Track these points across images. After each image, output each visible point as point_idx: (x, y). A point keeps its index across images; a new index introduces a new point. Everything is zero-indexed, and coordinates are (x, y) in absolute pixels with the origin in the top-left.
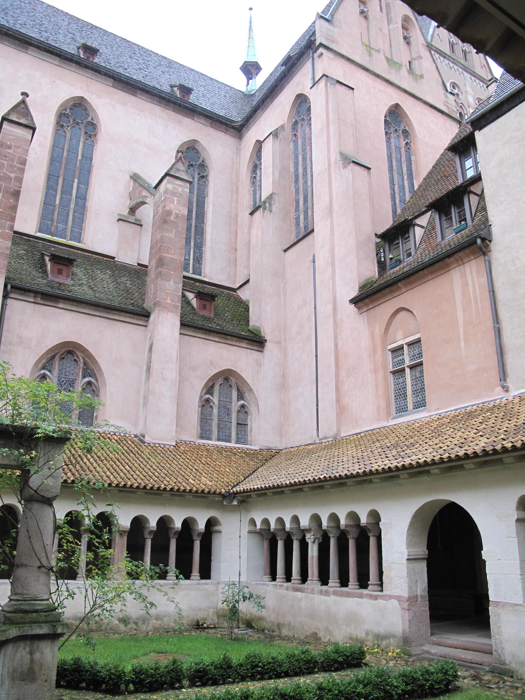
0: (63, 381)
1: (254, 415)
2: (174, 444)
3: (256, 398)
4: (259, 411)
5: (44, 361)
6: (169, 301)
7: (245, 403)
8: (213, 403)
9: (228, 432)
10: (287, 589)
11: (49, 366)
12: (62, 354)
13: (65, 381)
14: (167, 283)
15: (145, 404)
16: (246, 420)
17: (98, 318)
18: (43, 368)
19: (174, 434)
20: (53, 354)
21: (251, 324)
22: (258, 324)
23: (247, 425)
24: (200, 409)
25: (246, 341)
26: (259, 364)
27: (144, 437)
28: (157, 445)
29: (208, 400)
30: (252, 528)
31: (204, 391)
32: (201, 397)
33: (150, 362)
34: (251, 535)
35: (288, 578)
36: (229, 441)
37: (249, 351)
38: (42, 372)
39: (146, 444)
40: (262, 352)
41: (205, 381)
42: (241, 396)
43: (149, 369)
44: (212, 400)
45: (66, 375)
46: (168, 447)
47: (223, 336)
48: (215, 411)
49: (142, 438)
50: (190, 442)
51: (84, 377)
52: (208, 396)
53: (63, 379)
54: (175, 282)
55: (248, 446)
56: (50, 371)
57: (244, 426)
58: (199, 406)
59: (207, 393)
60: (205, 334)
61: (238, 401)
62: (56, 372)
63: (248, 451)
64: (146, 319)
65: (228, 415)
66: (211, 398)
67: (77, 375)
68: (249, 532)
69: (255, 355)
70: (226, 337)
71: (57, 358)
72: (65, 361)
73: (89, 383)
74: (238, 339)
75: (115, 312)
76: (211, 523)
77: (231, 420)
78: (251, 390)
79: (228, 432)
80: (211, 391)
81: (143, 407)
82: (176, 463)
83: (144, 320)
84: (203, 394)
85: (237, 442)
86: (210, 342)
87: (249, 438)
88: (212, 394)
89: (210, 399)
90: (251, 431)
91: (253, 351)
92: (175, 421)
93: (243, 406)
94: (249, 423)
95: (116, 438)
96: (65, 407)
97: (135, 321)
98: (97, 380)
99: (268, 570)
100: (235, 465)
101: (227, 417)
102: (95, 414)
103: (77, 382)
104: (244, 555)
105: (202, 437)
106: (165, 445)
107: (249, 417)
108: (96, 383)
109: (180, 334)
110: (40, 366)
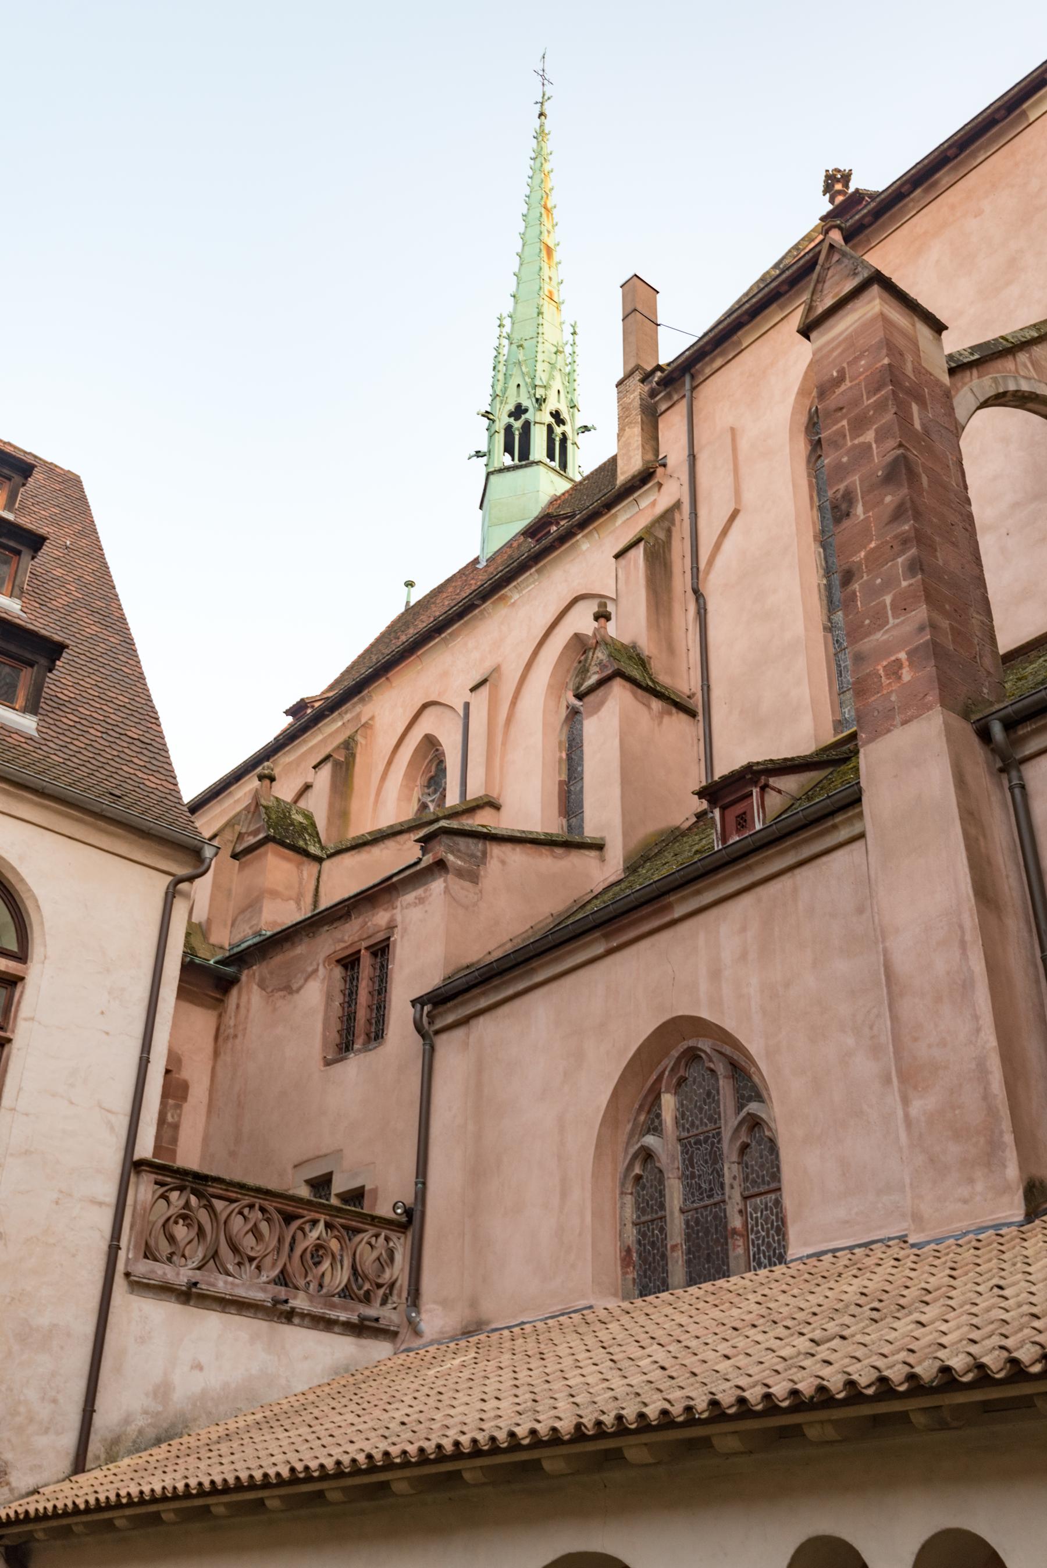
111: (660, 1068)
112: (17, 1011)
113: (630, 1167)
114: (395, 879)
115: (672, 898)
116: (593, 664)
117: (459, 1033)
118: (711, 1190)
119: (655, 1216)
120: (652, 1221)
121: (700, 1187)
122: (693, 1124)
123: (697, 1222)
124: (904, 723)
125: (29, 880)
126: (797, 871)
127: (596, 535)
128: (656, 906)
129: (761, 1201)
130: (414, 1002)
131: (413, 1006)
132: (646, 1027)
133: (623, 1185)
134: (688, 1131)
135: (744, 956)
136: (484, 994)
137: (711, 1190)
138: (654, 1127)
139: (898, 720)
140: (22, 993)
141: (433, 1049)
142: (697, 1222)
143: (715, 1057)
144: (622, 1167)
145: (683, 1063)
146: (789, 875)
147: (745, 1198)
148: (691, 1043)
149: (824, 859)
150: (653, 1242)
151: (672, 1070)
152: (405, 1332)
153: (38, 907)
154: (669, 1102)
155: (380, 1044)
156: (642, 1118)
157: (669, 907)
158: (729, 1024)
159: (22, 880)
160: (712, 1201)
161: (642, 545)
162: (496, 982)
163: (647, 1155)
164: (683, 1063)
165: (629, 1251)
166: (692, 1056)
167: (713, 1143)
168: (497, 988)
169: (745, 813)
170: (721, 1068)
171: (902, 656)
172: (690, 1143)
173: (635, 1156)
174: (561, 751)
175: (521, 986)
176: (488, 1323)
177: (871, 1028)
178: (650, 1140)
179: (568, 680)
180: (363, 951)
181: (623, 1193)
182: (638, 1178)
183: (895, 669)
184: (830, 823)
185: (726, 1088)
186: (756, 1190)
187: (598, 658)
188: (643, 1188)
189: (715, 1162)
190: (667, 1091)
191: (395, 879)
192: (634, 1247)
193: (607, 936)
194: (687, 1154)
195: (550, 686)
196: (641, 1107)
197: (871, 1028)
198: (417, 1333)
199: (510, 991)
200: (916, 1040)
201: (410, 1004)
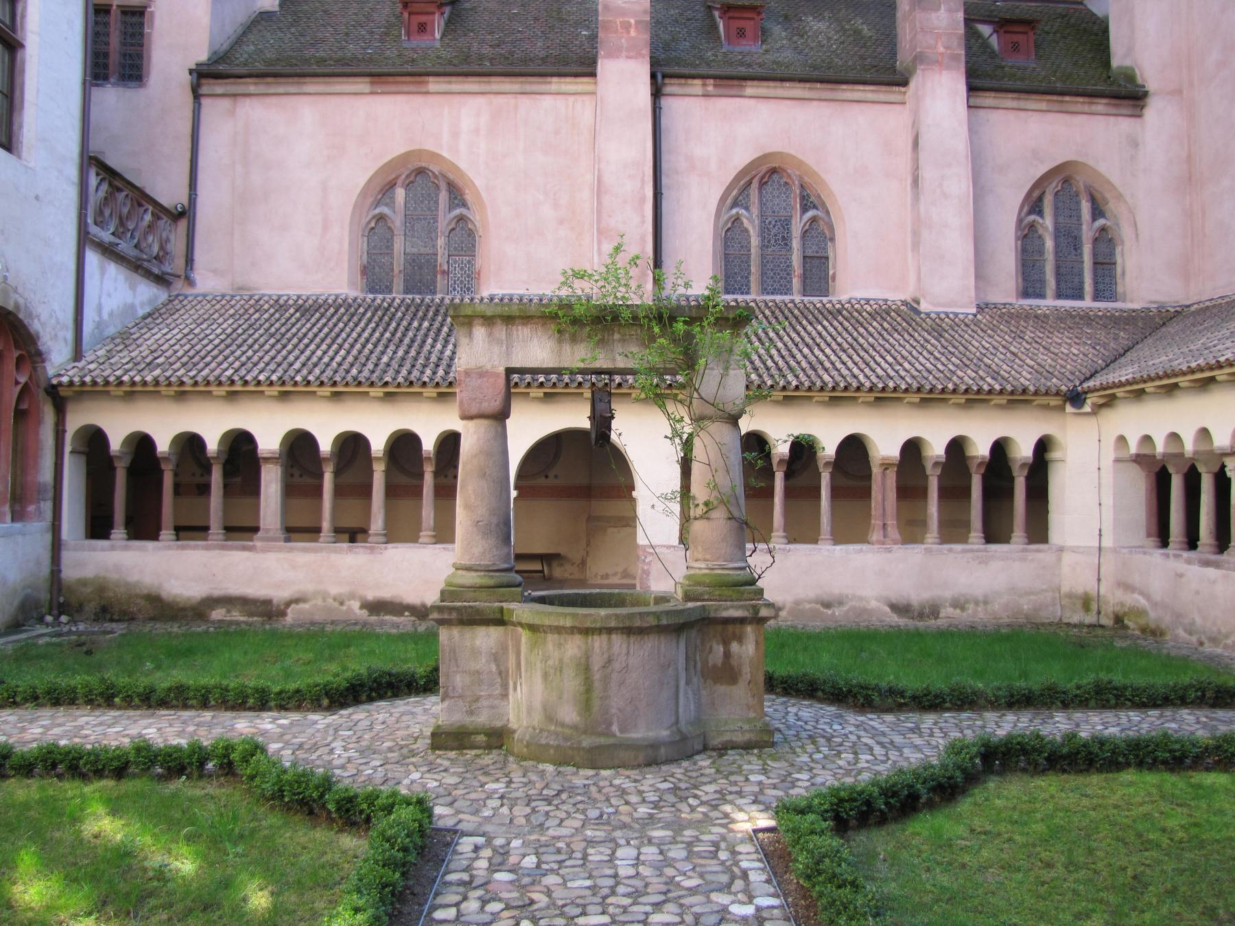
0: (770, 223)
1: (1127, 244)
2: (974, 311)
3: (1130, 211)
4: (1137, 235)
5: (734, 193)
6: (941, 49)
7: (1109, 223)
8: (1046, 229)
9: (1076, 280)
10: (1189, 562)
11: (744, 199)
12: (763, 177)
13: (773, 223)
14: (933, 15)
15: (916, 245)
16: (1112, 254)
17: (815, 103)
18: (735, 204)
19: (973, 293)
20: (747, 178)
21: (1115, 63)
22: (1127, 63)
23: (1115, 264)
24: (1019, 242)
25: (1104, 101)
26: (1134, 143)
27: (918, 303)
28: (943, 316)
29: (1032, 226)
30: (1124, 455)
31: (1026, 209)
32: (1020, 221)
33: (918, 167)
34: (1120, 465)
35: (1192, 542)
36: (1080, 297)
37: (1112, 119)
38: (734, 211)
39: (922, 315)
40: (1140, 116)
41: (1026, 190)
42: (1097, 212)
43: (916, 181)
44: (1041, 225)
45: (774, 212)
46: (961, 316)
47: (1055, 98)
48: (1049, 244)
49: (915, 306)
50: (1005, 304)
51: (805, 209)
52: (1032, 217)
53: (770, 219)
54: (950, 11)
55: (1118, 305)
56: (747, 209)
57: (1108, 266)
58: (1017, 239)
59: (1030, 213)
60: (1019, 99)
61: (1094, 220)
62: (755, 211)
63: (1117, 314)
64: (903, 89)
65: (1075, 249)
66: (1041, 221)
67: (793, 208)
68: (1117, 461)
69: (1125, 125)
70: (1060, 98)
71: (755, 184)
72: (769, 188)
73: (814, 220)
74: (1086, 100)
75: (844, 87)
76: (1043, 446)
77: (1082, 258)
78: (1120, 197)
79: (1076, 280)
80: (1038, 206)
81: (913, 250)
82: (976, 344)
83: (900, 92)
84: (1023, 214)
85: (1096, 298)
86: (1030, 113)
87: (1120, 289)
88: (1040, 213)
89: (1038, 223)
90: (1123, 273)
91: (1120, 119)
92: (972, 270)
93: (1103, 229)
94: (1119, 260)
95: (869, 309)
96: (779, 266)
97: (882, 97)
98: (828, 212)
99: (1154, 529)
100: (1089, 342)
101: (1074, 252)
102: (831, 273)
103: (793, 222)
104: (1108, 501)
105: (1025, 294)
106: (956, 315)
107: (1118, 250)
108: (826, 218)
109: (969, 107)
110: (729, 201)
113: (369, 222)
124: (628, 57)
128: (418, 79)
131: (190, 74)
133: (364, 231)
135: (477, 131)
138: (391, 204)
139: (624, 54)
141: (200, 104)
143: (441, 179)
144: (364, 221)
154: (400, 193)
162: (269, 80)
170: (443, 186)
171: (632, 21)
173: (374, 217)
177: (555, 194)
181: (363, 236)
183: (627, 27)
185: (443, 196)
186: (456, 253)
189: (430, 232)
197: (555, 194)
200: (610, 216)
201: (187, 72)
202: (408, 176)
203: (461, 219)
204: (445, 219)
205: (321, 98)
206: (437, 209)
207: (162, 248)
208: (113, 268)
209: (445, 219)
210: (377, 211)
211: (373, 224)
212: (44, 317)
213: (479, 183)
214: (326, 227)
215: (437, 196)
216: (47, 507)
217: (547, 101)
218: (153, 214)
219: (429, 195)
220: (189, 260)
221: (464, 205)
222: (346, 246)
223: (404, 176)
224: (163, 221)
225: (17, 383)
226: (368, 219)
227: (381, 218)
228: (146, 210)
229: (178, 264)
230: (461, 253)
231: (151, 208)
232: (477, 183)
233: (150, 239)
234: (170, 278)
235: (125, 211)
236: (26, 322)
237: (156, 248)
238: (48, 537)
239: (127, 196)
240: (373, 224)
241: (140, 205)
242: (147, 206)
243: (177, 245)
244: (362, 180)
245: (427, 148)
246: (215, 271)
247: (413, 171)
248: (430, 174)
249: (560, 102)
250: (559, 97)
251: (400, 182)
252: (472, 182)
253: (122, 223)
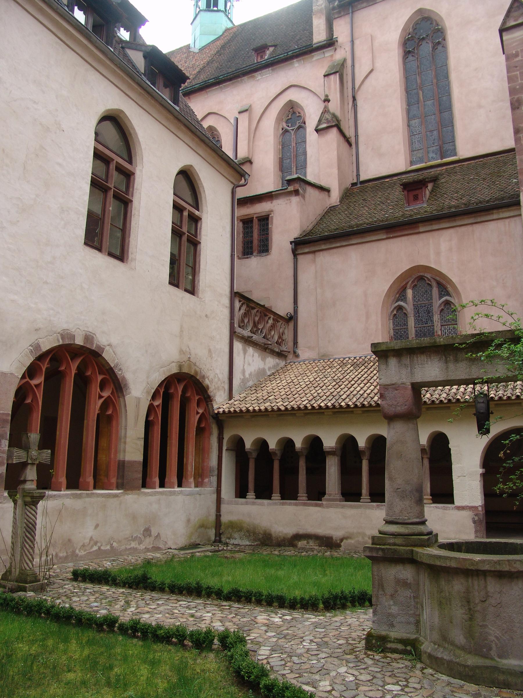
111: (407, 281)
112: (200, 232)
114: (273, 193)
115: (420, 225)
116: (323, 119)
117: (310, 256)
118: (427, 321)
119: (401, 327)
120: (401, 329)
121: (422, 320)
122: (419, 300)
123: (421, 331)
125: (202, 180)
126: (474, 225)
127: (302, 62)
129: (448, 327)
130: (291, 243)
132: (406, 267)
134: (417, 302)
135: (450, 249)
136: (324, 244)
137: (427, 321)
140: (201, 224)
142: (421, 331)
143: (432, 280)
145: (416, 280)
146: (471, 225)
147: (441, 326)
148: (421, 274)
149: (486, 223)
150: (401, 335)
151: (412, 282)
152: (291, 356)
153: (204, 191)
154: (410, 293)
155: (268, 255)
156: (397, 296)
157: (418, 227)
158: (444, 271)
159: (200, 179)
160: (427, 325)
161: (338, 74)
163: (400, 308)
164: (416, 280)
165: (392, 337)
166: (421, 278)
167: (428, 307)
168: (331, 243)
169: (417, 195)
170: (434, 284)
172: (418, 306)
173: (395, 308)
174: (280, 146)
175: (344, 244)
176: (333, 355)
177: (503, 280)
178: (401, 303)
179: (283, 117)
180: (255, 218)
181: (389, 319)
182: (395, 315)
184: (492, 212)
185: (435, 291)
186: (446, 324)
187: (326, 117)
188: (397, 318)
189: (429, 313)
190: (410, 288)
191: (273, 193)
192: (393, 336)
193: (387, 233)
194: (416, 309)
195: (277, 118)
196: (398, 292)
197: (503, 280)
198: (297, 356)
199: (338, 245)
202: (413, 282)
203: (447, 303)
204: (437, 303)
205: (360, 246)
206: (431, 299)
207: (280, 337)
208: (251, 350)
209: (437, 303)
210: (397, 304)
211: (395, 312)
212: (211, 376)
213: (455, 280)
214: (368, 316)
215: (431, 291)
216: (214, 479)
217: (492, 225)
218: (273, 319)
219: (426, 291)
220: (295, 343)
221: (448, 294)
222: (380, 326)
223: (410, 282)
224: (280, 323)
225: (198, 413)
226: (392, 309)
227: (400, 308)
228: (269, 318)
229: (288, 346)
230: (448, 323)
231: (272, 316)
232: (454, 280)
233: (273, 333)
234: (286, 354)
235: (257, 319)
236: (201, 381)
237: (276, 338)
238: (215, 496)
239: (258, 311)
240: (395, 312)
241: (266, 315)
242: (270, 315)
243: (288, 336)
244: (387, 288)
245: (422, 264)
246: (309, 348)
247: (415, 279)
248: (426, 279)
249: (500, 223)
250: (499, 221)
251: (408, 286)
252: (451, 280)
253: (255, 325)
